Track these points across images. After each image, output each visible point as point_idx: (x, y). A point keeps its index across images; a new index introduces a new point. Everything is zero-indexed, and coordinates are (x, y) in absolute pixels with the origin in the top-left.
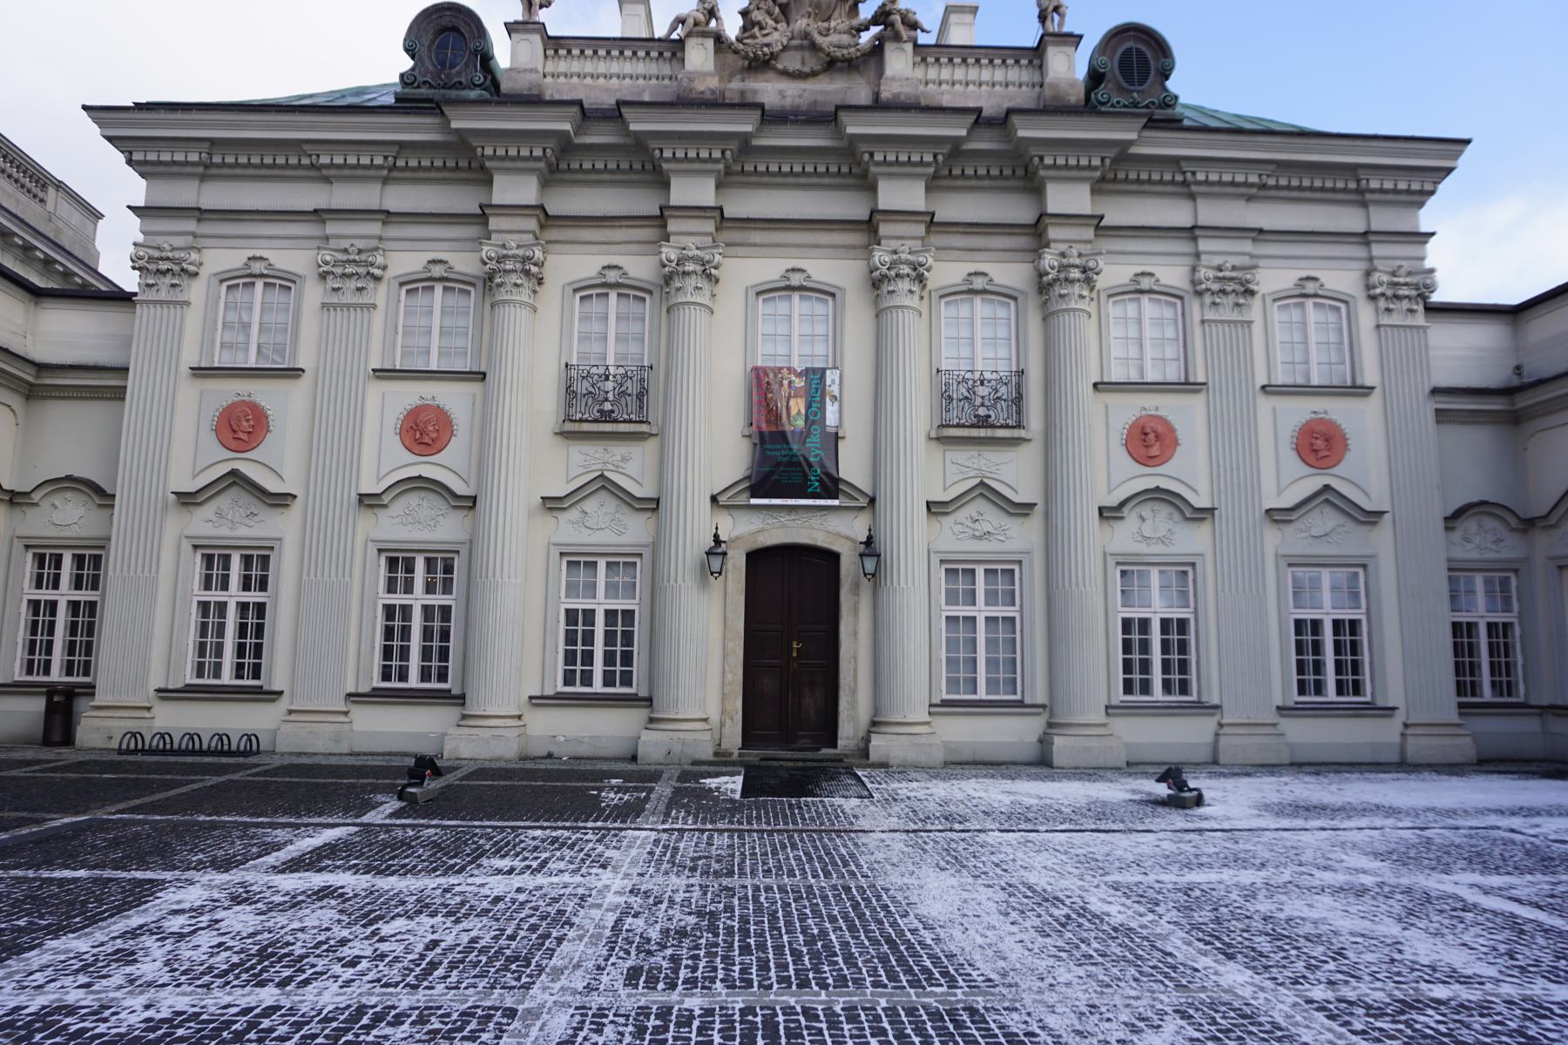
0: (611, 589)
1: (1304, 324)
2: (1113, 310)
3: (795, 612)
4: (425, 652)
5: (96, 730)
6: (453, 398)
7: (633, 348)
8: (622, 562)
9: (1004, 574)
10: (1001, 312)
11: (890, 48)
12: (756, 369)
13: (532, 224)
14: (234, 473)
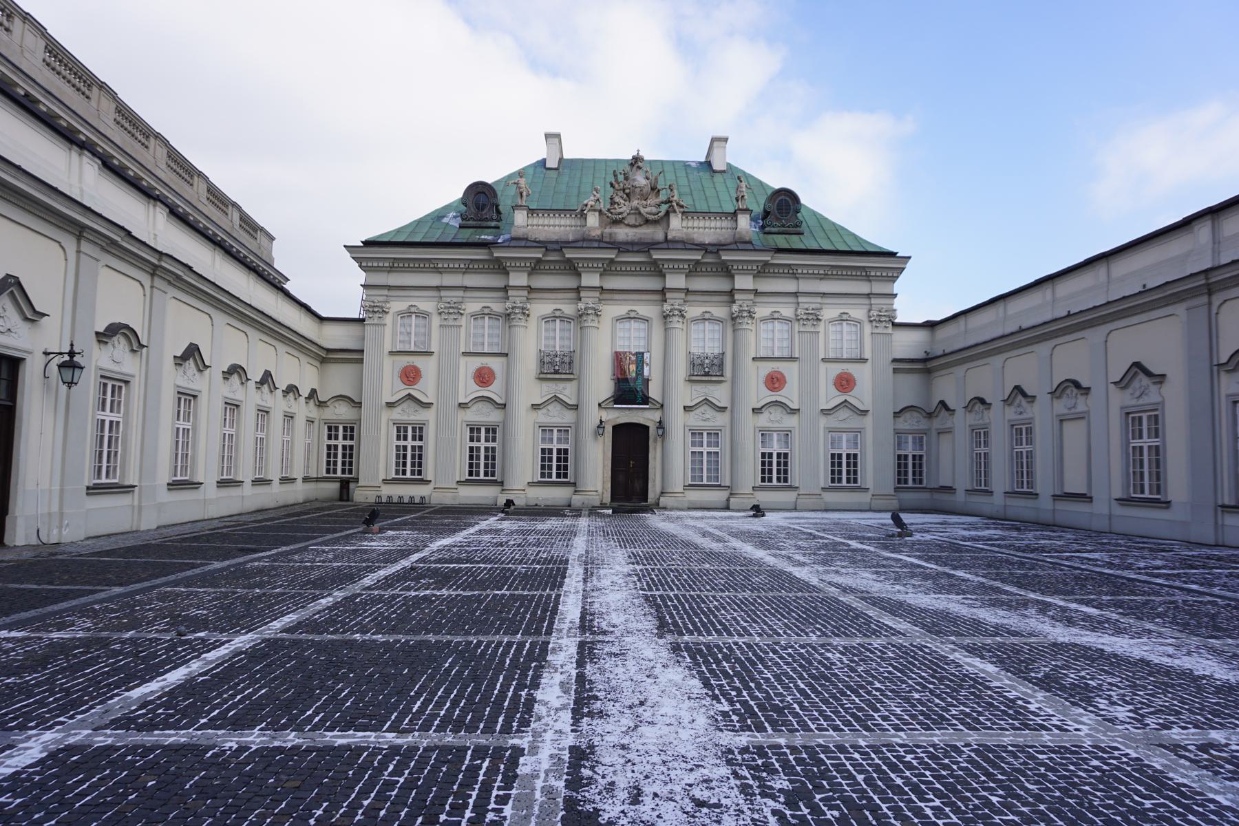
0: (559, 441)
1: (842, 332)
2: (763, 326)
3: (631, 449)
4: (485, 464)
5: (362, 495)
6: (495, 364)
7: (566, 343)
8: (564, 430)
9: (714, 435)
10: (716, 327)
11: (672, 215)
12: (616, 353)
13: (525, 293)
14: (409, 394)
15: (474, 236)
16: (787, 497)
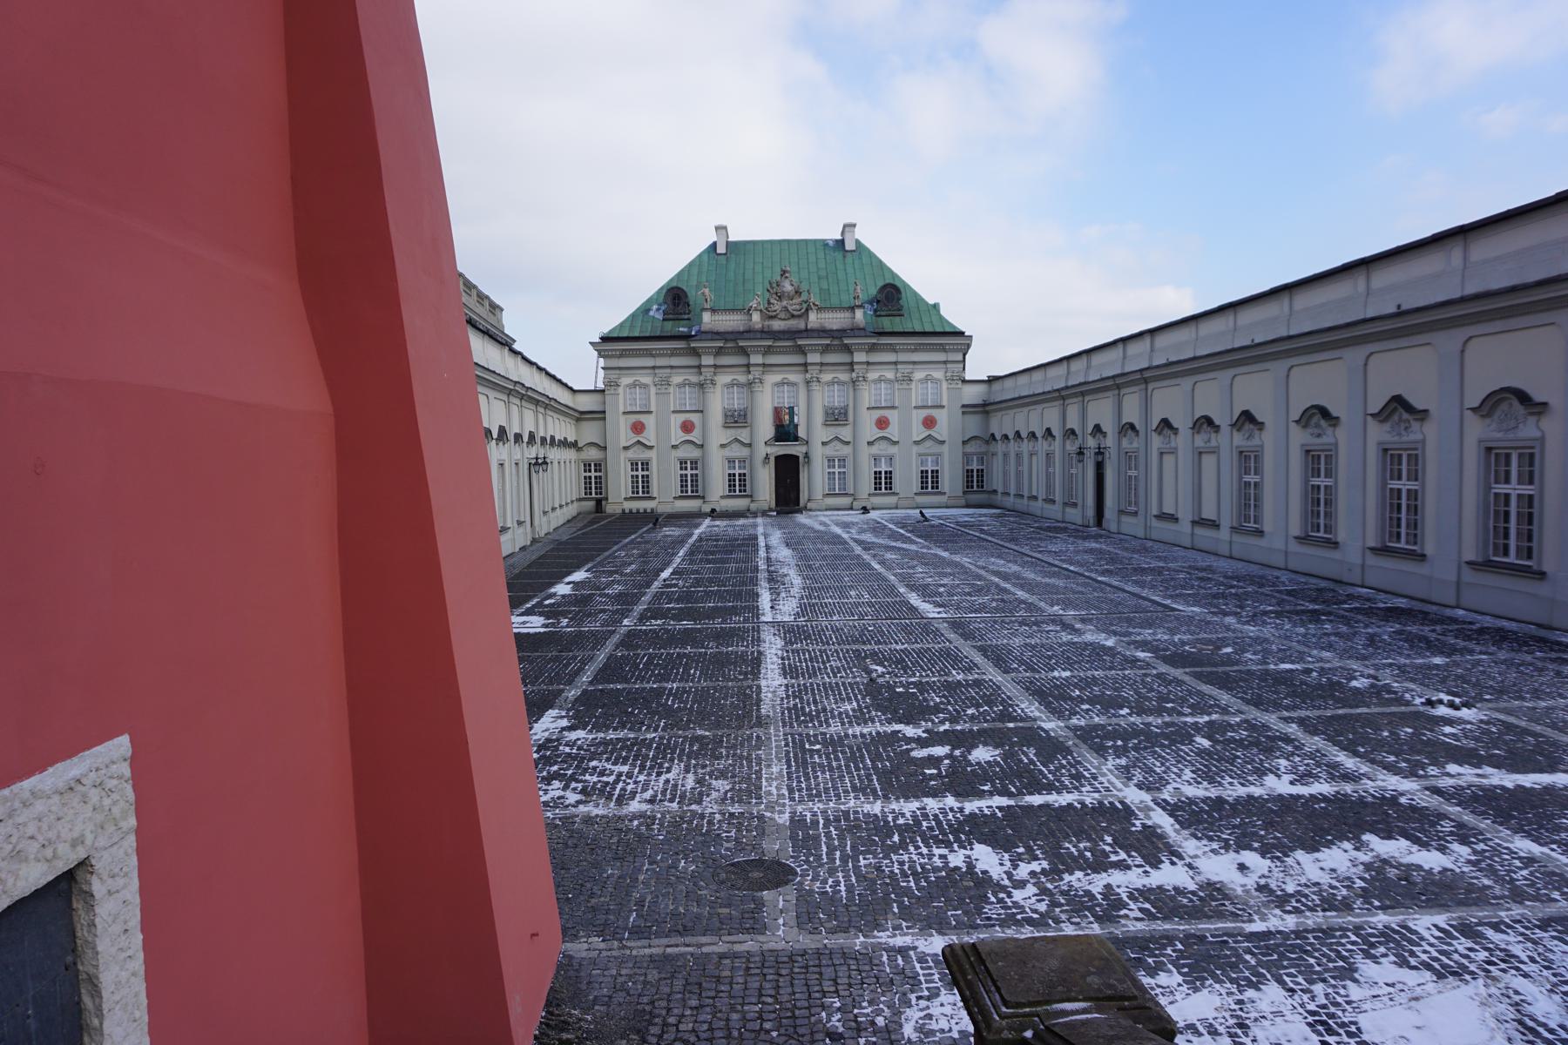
3: (788, 472)
4: (692, 485)
5: (610, 508)
6: (695, 418)
9: (842, 460)
15: (672, 325)
16: (892, 500)
